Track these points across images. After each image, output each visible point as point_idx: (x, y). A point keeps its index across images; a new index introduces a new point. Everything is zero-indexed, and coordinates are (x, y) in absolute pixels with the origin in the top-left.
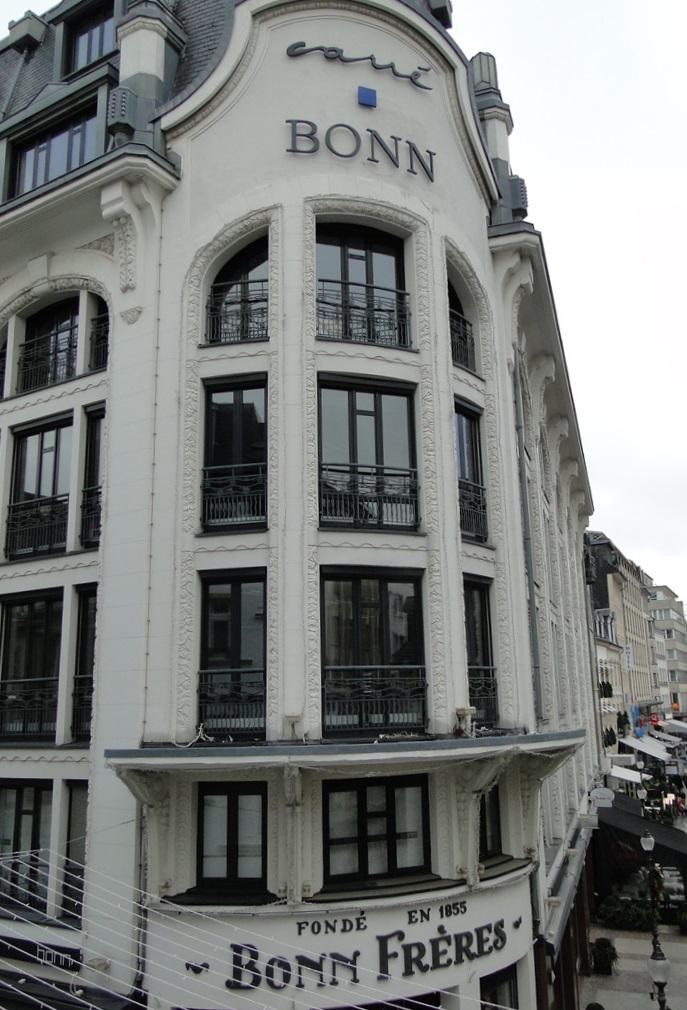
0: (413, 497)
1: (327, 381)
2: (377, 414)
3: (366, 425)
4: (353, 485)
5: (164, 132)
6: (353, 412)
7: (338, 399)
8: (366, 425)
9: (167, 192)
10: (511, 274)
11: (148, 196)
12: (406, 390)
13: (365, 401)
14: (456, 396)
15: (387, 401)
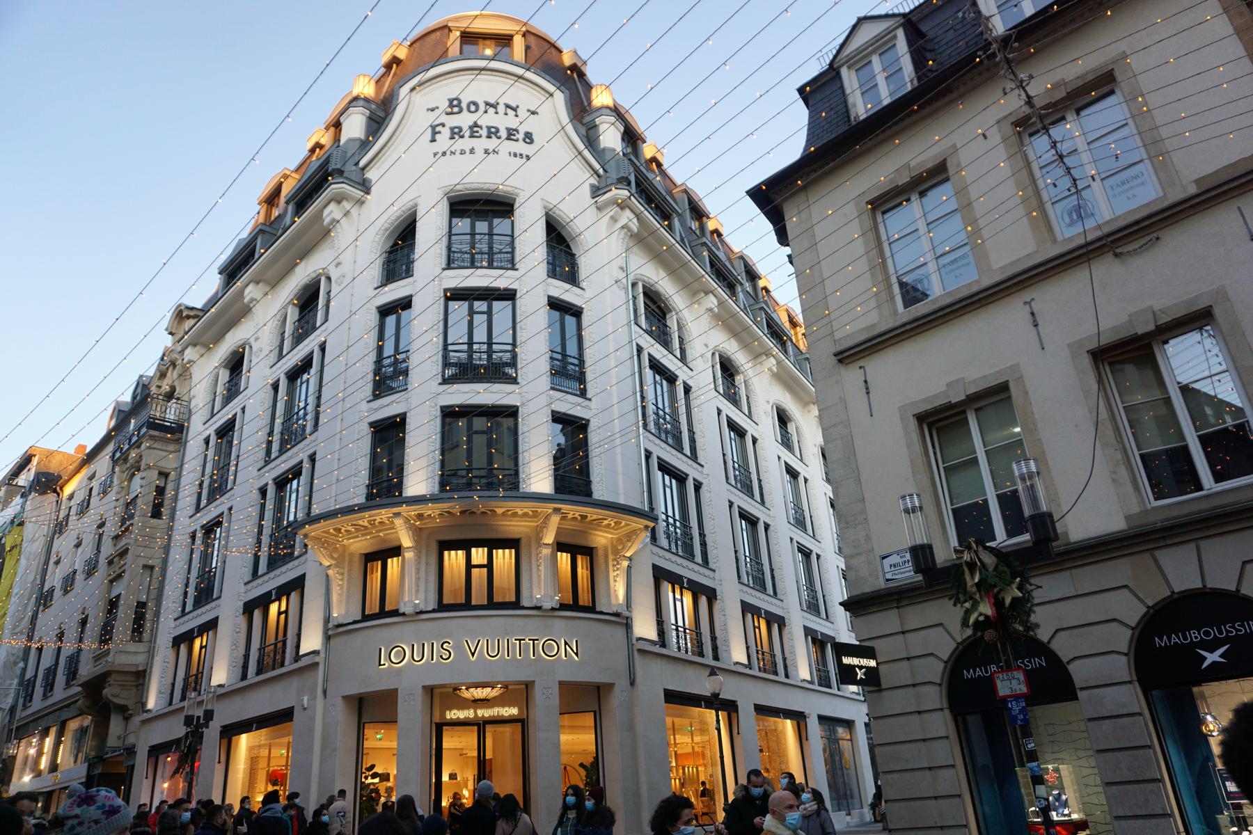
0: (513, 363)
1: (455, 295)
2: (489, 313)
3: (480, 320)
4: (470, 357)
5: (363, 169)
6: (472, 313)
7: (459, 309)
8: (480, 320)
9: (361, 202)
10: (614, 219)
11: (346, 205)
12: (509, 295)
13: (480, 306)
14: (549, 297)
15: (497, 305)
